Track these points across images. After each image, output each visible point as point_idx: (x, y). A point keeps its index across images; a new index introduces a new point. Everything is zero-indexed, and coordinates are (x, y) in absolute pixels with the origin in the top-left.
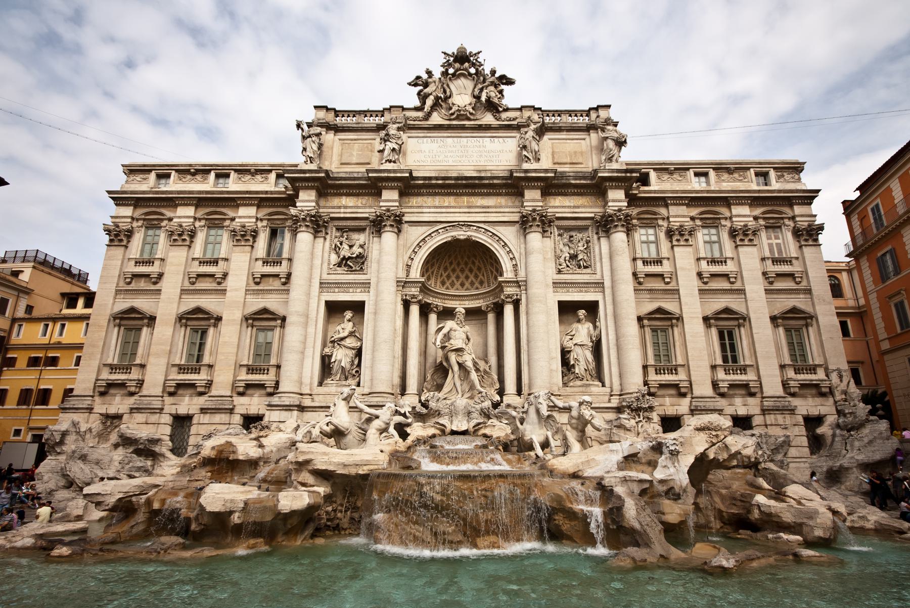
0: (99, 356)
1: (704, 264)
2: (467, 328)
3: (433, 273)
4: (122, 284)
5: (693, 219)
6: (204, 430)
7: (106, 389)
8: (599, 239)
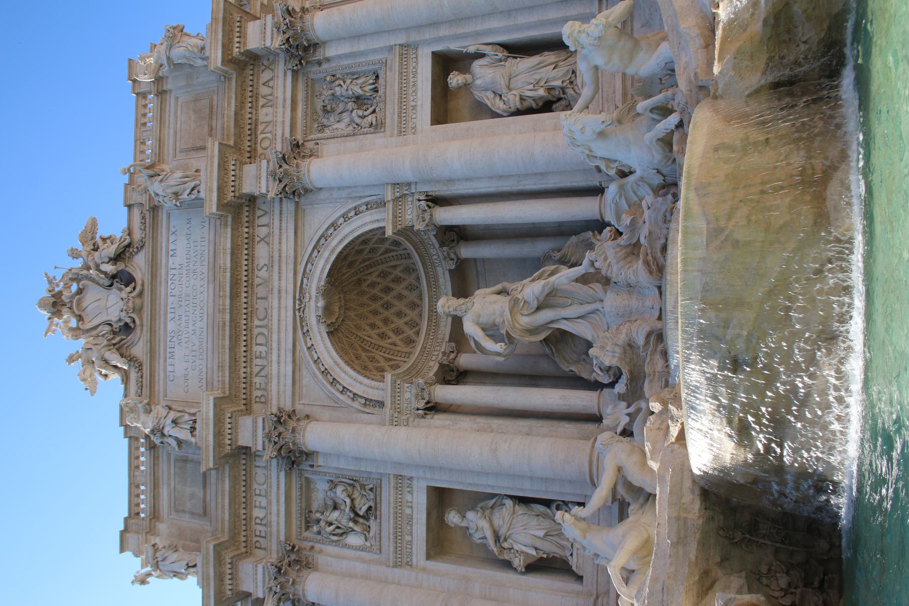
2: (477, 292)
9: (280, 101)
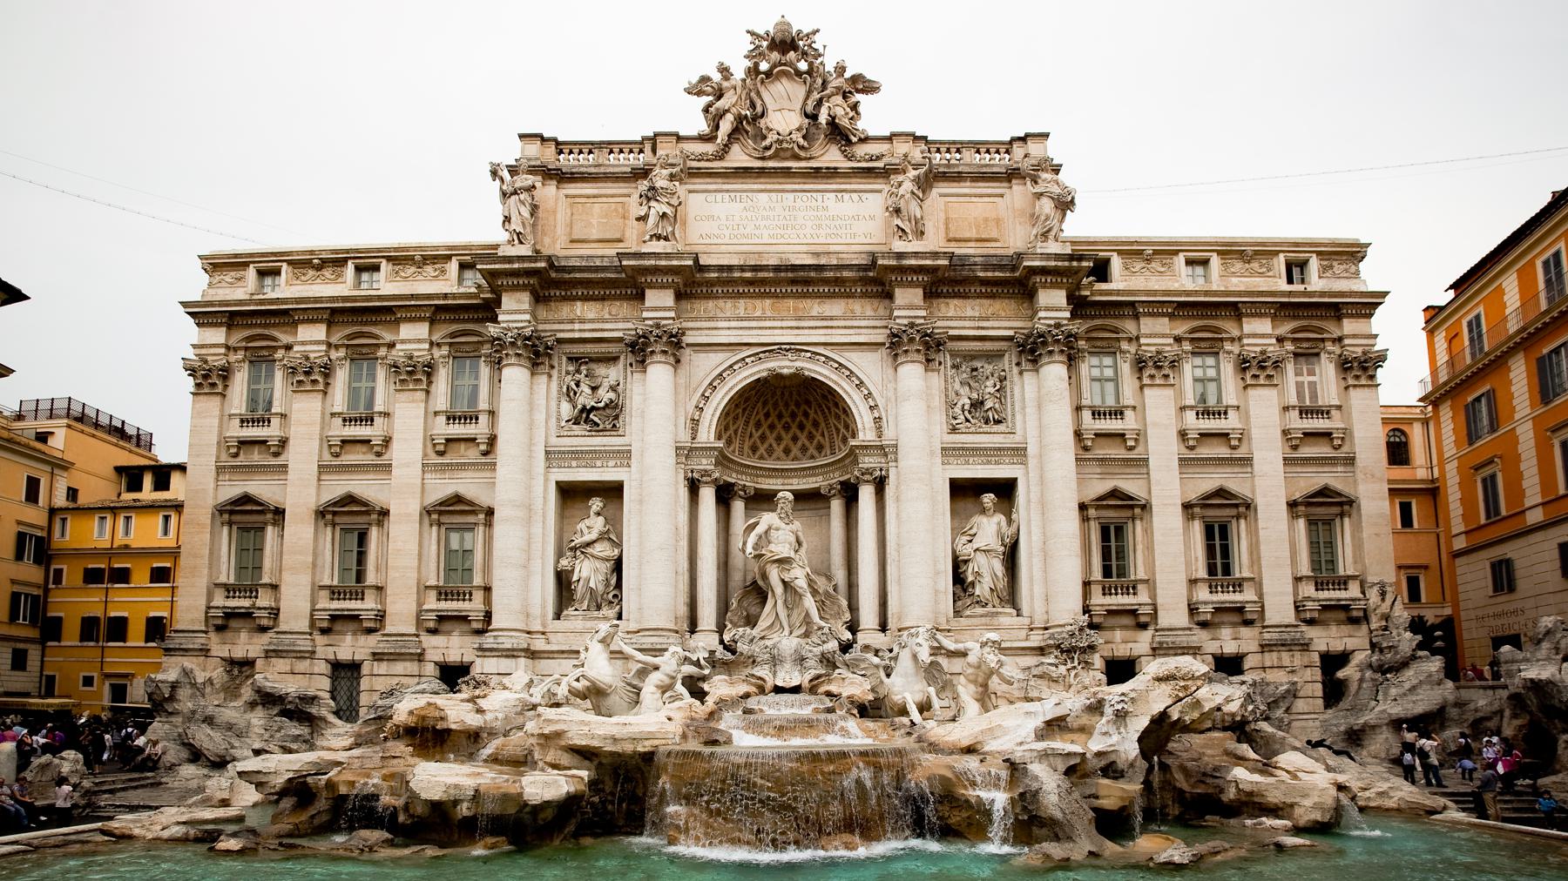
0: (206, 571)
2: (797, 525)
3: (736, 432)
4: (224, 456)
5: (1178, 340)
7: (225, 622)
8: (1021, 373)
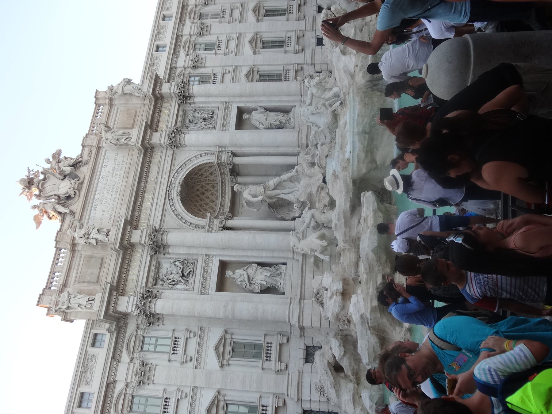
1: (218, 52)
6: (316, 396)
8: (194, 103)
9: (172, 114)
